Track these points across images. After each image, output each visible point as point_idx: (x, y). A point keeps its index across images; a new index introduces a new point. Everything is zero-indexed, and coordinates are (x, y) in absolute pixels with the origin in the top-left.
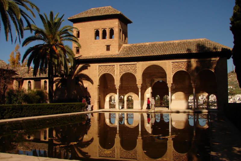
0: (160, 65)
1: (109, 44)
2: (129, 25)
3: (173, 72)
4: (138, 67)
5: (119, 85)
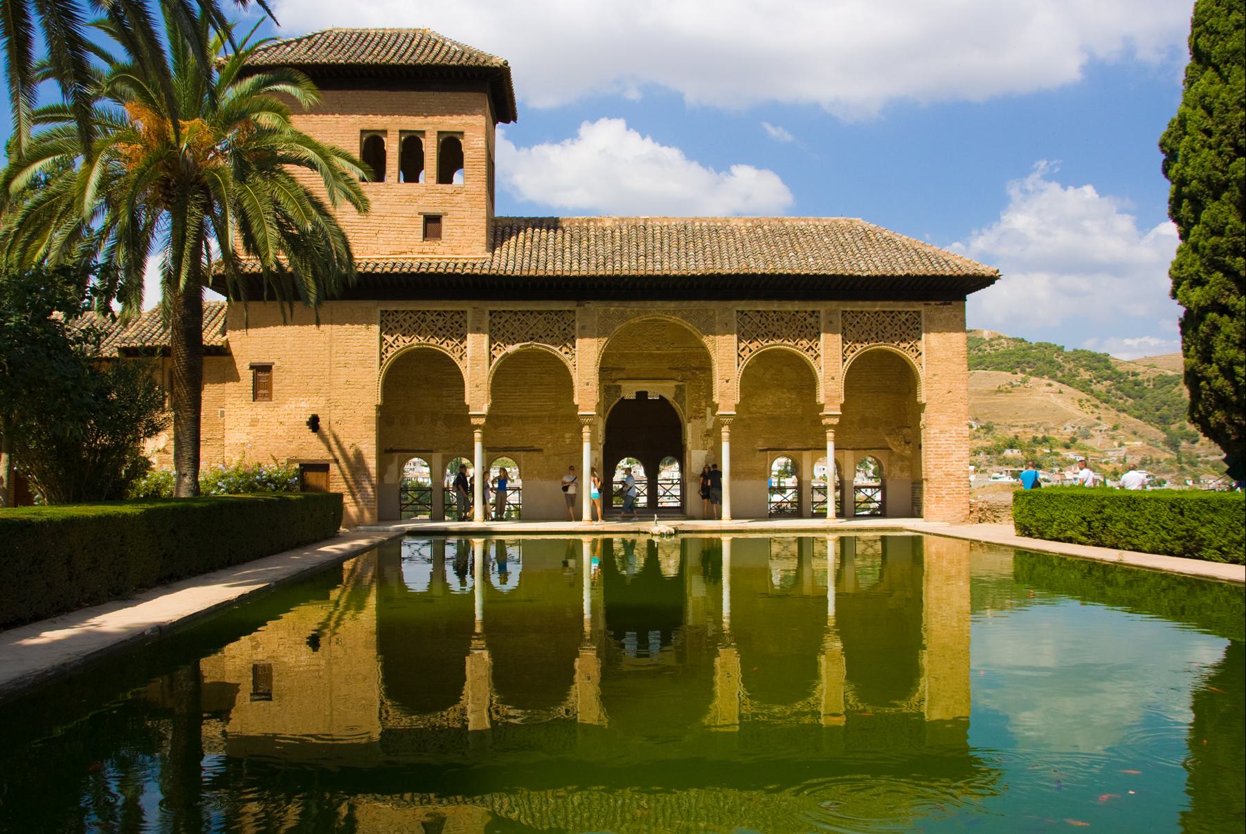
4: (583, 328)
5: (485, 411)
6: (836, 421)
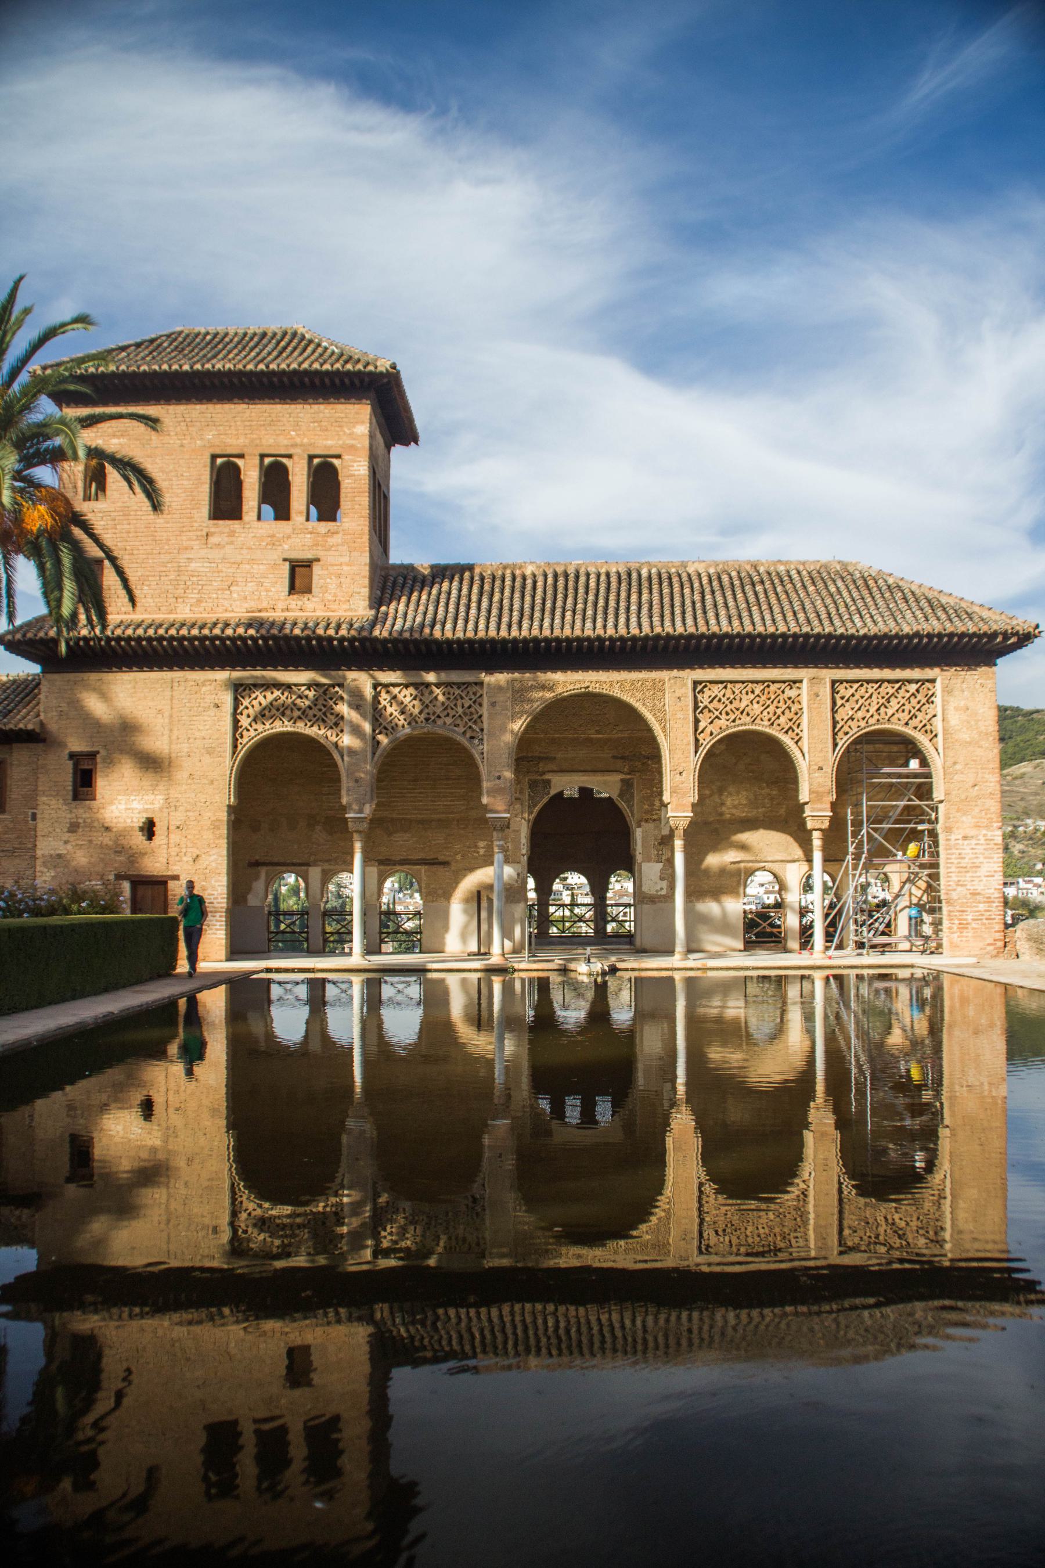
0: (626, 697)
1: (309, 556)
2: (397, 450)
3: (700, 737)
4: (493, 704)
6: (826, 825)
